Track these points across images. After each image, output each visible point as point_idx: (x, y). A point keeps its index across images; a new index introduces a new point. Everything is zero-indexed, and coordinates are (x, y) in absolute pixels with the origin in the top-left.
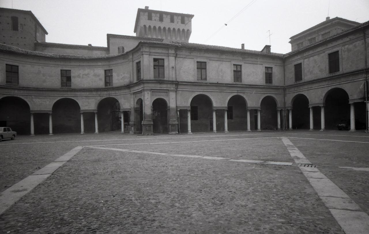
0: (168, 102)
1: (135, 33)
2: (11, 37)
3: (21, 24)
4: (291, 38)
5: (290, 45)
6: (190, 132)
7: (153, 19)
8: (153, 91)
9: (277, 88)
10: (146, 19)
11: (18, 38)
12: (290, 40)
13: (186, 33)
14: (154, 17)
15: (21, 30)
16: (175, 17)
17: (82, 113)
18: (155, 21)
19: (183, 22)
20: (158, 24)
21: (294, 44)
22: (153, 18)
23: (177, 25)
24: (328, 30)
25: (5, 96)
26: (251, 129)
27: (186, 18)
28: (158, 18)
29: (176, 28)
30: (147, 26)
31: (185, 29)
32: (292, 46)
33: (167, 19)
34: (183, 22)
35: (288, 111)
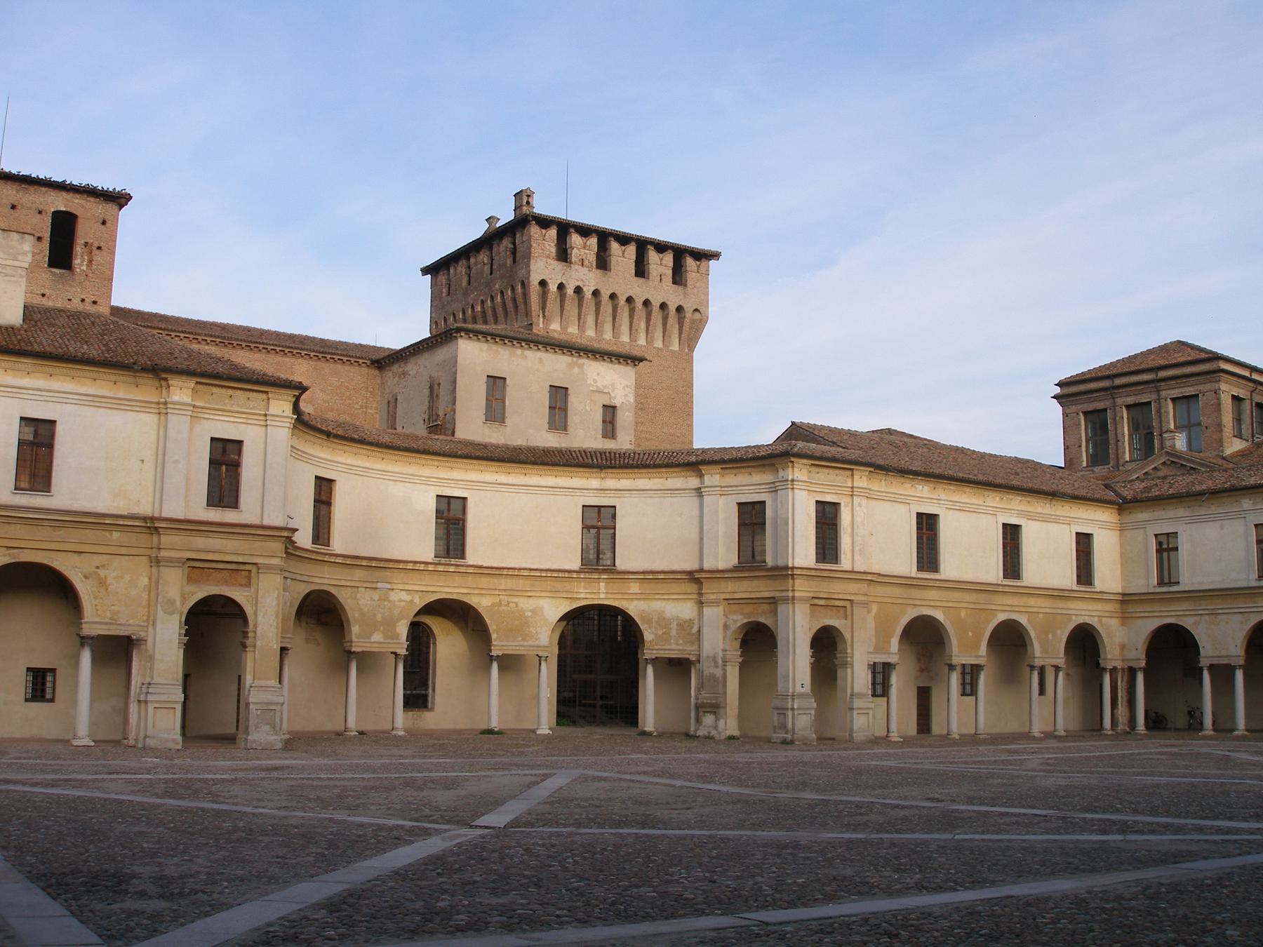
0: (847, 636)
1: (429, 276)
2: (43, 295)
3: (86, 244)
4: (1060, 384)
5: (1057, 409)
6: (895, 734)
7: (574, 259)
8: (815, 604)
9: (1100, 597)
10: (548, 257)
11: (70, 300)
12: (1058, 390)
13: (687, 322)
14: (578, 249)
15: (84, 268)
16: (653, 256)
17: (498, 656)
18: (583, 265)
19: (678, 275)
20: (588, 278)
21: (1074, 408)
22: (575, 254)
23: (659, 288)
24: (1191, 389)
25: (317, 588)
26: (1147, 727)
27: (690, 262)
28: (591, 257)
29: (654, 303)
30: (553, 287)
31: (685, 306)
32: (1065, 415)
33: (623, 258)
34: (678, 275)
35: (1132, 672)
